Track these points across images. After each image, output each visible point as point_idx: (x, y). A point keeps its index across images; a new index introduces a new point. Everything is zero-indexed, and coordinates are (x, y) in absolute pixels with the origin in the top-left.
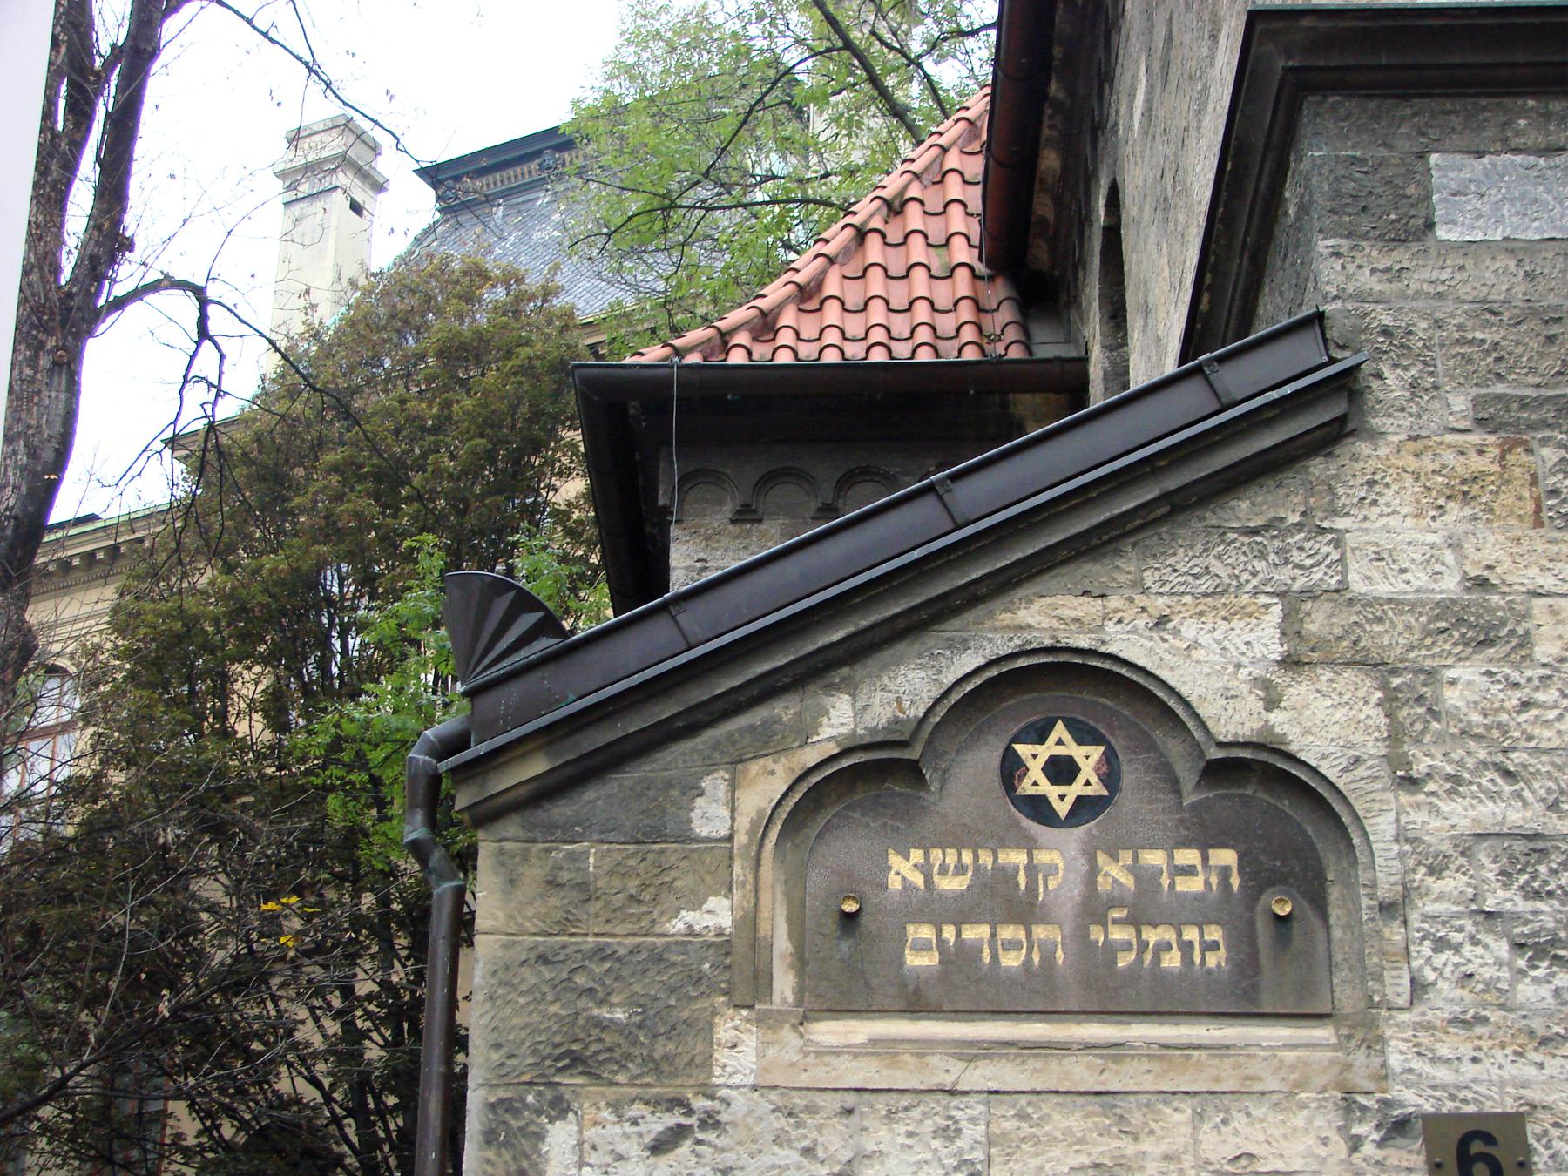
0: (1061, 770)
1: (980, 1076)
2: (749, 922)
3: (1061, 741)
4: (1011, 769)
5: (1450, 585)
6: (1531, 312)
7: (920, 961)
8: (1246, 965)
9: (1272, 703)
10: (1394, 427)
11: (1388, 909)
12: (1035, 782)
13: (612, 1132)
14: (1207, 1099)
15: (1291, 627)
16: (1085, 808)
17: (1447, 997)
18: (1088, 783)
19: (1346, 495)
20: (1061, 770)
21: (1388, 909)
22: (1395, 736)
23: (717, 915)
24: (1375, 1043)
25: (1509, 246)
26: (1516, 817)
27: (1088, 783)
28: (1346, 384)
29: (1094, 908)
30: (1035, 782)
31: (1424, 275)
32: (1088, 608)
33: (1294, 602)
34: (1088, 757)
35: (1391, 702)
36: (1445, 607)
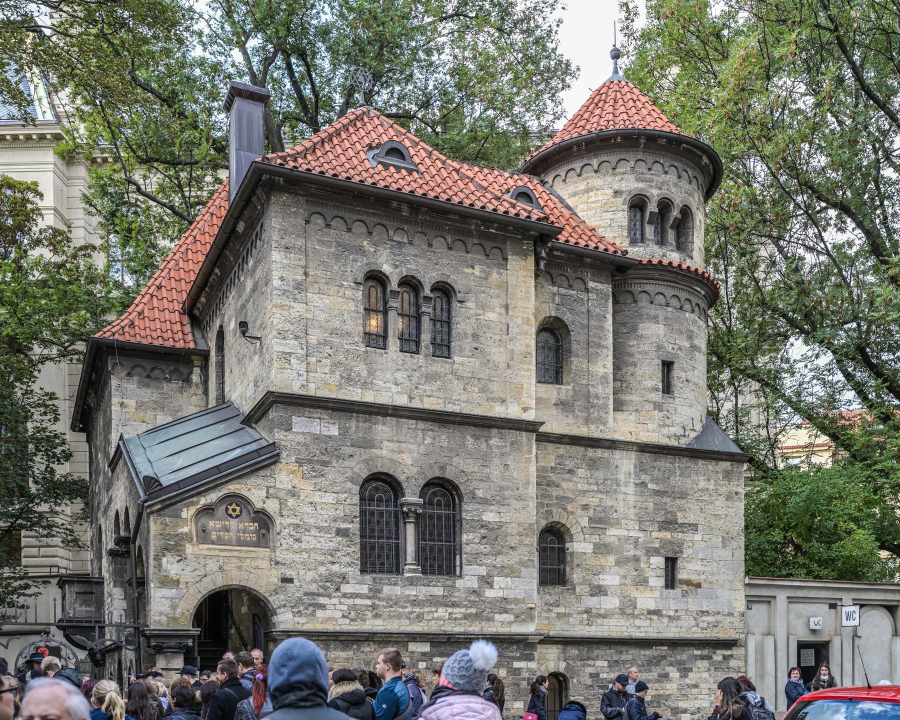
5: (290, 487)
6: (305, 444)
8: (259, 539)
9: (264, 503)
11: (278, 534)
14: (253, 559)
15: (267, 492)
17: (285, 546)
21: (278, 534)
22: (281, 509)
24: (275, 552)
25: (303, 433)
26: (296, 522)
31: (290, 437)
33: (268, 488)
35: (280, 504)
36: (289, 490)
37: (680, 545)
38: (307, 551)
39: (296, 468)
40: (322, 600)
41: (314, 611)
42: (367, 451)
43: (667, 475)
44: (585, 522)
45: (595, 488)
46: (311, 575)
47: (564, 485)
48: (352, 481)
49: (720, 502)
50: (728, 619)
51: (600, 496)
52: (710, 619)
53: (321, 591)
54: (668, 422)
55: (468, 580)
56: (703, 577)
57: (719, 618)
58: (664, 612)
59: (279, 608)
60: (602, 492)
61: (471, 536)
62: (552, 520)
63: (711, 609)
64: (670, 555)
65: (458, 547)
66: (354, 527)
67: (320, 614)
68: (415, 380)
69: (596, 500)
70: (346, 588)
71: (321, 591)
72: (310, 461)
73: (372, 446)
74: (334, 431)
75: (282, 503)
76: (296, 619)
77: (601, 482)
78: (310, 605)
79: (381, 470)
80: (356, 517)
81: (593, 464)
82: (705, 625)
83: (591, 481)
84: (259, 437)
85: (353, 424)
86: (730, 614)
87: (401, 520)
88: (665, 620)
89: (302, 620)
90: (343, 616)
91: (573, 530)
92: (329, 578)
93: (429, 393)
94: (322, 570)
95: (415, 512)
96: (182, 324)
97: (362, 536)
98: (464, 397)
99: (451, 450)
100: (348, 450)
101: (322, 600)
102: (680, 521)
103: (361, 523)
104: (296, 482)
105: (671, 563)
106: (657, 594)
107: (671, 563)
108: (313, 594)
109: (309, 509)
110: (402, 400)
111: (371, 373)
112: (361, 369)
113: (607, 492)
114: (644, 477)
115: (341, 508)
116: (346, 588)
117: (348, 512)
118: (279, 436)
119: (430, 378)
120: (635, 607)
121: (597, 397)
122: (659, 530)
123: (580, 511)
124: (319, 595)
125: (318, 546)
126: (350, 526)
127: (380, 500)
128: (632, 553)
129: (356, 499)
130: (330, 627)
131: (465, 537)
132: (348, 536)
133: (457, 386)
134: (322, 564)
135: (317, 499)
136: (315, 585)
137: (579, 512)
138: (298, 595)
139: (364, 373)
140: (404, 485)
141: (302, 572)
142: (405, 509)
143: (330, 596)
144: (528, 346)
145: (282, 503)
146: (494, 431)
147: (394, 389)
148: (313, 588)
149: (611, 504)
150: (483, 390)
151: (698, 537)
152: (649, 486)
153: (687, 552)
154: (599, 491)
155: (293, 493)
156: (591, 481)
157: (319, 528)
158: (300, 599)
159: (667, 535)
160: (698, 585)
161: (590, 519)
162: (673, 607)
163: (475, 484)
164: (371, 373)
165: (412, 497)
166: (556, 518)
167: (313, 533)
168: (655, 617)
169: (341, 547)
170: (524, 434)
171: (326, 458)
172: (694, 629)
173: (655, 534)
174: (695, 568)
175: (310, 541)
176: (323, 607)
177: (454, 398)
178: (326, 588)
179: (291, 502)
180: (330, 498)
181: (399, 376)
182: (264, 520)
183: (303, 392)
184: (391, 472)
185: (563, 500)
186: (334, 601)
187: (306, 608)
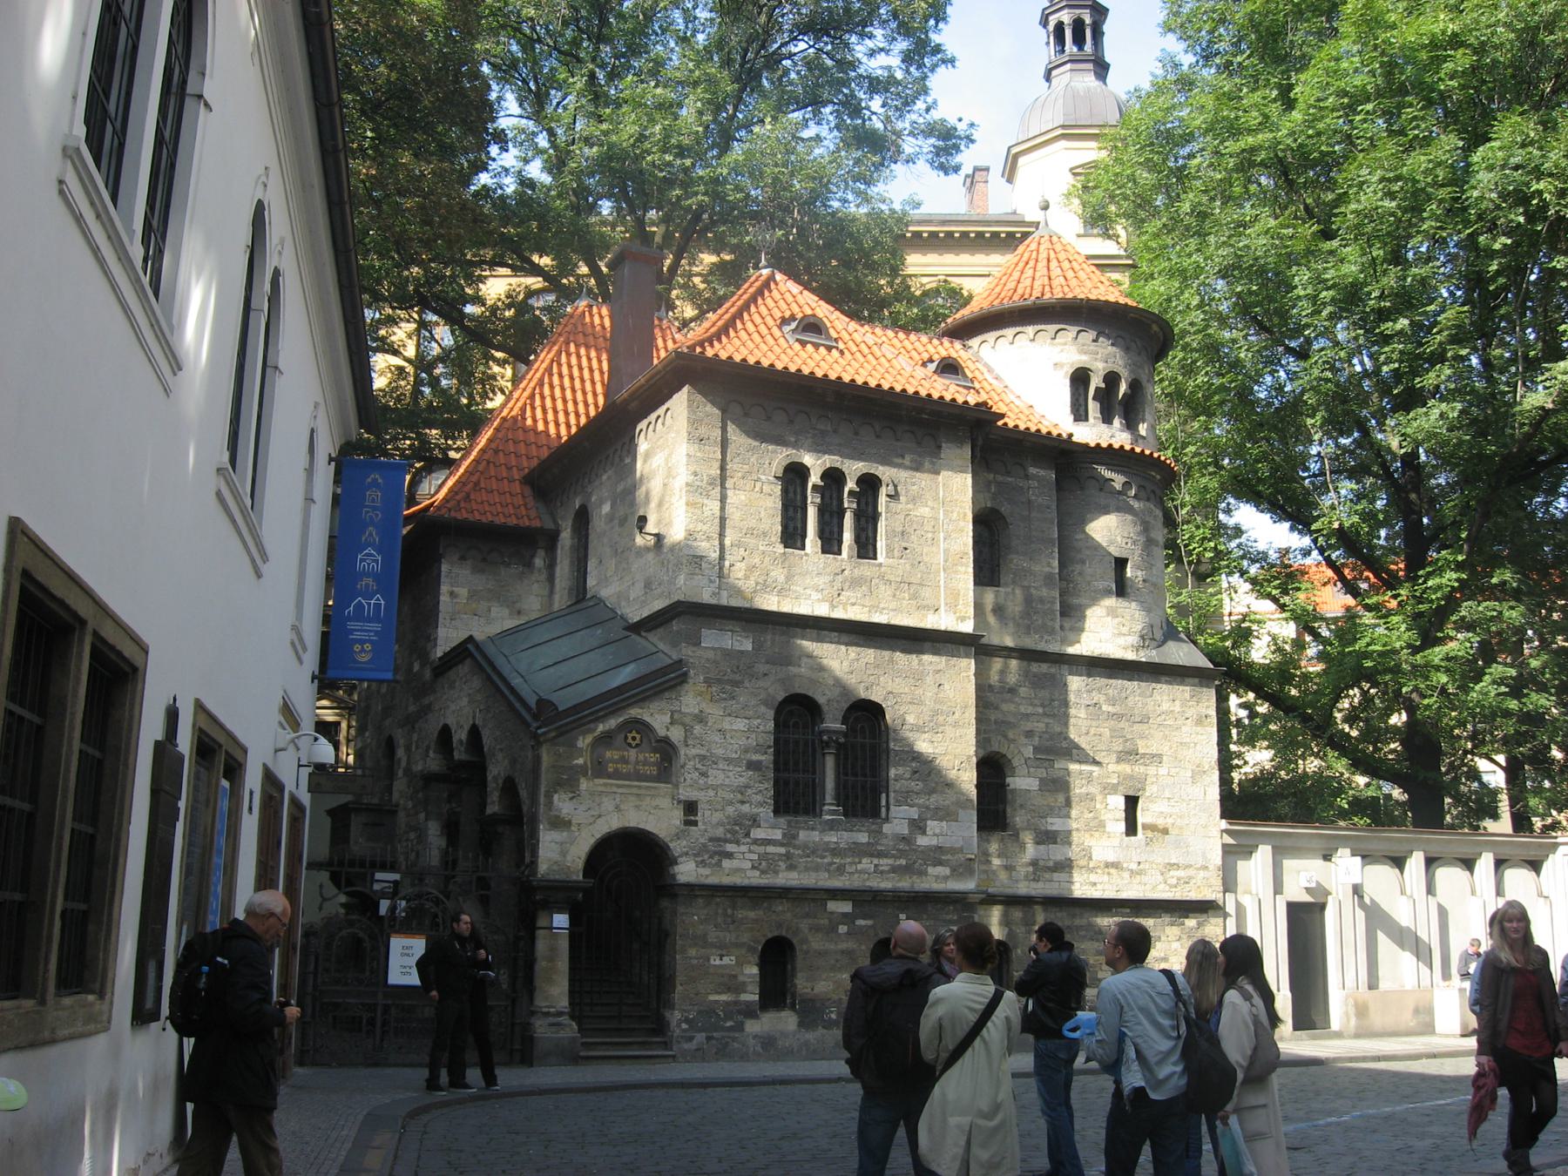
0: (634, 738)
1: (620, 790)
2: (585, 763)
3: (634, 734)
4: (626, 738)
5: (697, 711)
7: (610, 770)
8: (659, 774)
10: (691, 681)
12: (630, 740)
13: (564, 796)
15: (672, 717)
16: (637, 745)
17: (688, 783)
18: (638, 741)
19: (683, 693)
20: (634, 738)
23: (580, 761)
25: (713, 649)
27: (638, 741)
28: (685, 674)
29: (637, 763)
30: (630, 740)
31: (699, 653)
32: (640, 711)
34: (638, 736)
36: (696, 715)
37: (1143, 780)
38: (715, 788)
39: (704, 689)
40: (730, 847)
41: (720, 861)
42: (784, 668)
43: (1124, 695)
44: (1028, 752)
45: (1040, 710)
46: (717, 816)
47: (1005, 707)
48: (765, 703)
49: (1188, 728)
50: (1202, 874)
51: (1046, 720)
52: (1181, 873)
53: (729, 836)
54: (1125, 630)
55: (898, 820)
56: (1170, 821)
57: (1191, 872)
58: (1125, 865)
59: (680, 856)
60: (1048, 716)
61: (901, 770)
62: (989, 749)
63: (1181, 861)
64: (1131, 793)
65: (884, 783)
66: (767, 758)
67: (726, 863)
68: (838, 585)
69: (1041, 726)
70: (758, 833)
71: (729, 836)
72: (719, 681)
73: (789, 664)
74: (748, 646)
75: (688, 730)
76: (703, 871)
77: (1047, 703)
78: (716, 853)
79: (799, 691)
80: (769, 747)
81: (1038, 682)
82: (1174, 881)
83: (1036, 702)
84: (655, 650)
85: (769, 637)
86: (1205, 868)
87: (819, 750)
88: (1126, 875)
89: (707, 871)
90: (753, 867)
91: (1015, 762)
92: (738, 821)
93: (853, 600)
94: (730, 810)
95: (836, 742)
96: (523, 497)
97: (777, 770)
98: (893, 605)
99: (878, 666)
100: (761, 668)
101: (730, 847)
102: (1141, 751)
103: (777, 754)
104: (704, 705)
105: (1132, 802)
106: (1116, 842)
107: (1132, 802)
108: (718, 840)
109: (717, 738)
110: (822, 610)
111: (789, 578)
112: (778, 574)
113: (1054, 716)
114: (1097, 697)
115: (753, 736)
116: (758, 833)
117: (761, 741)
118: (686, 652)
119: (856, 583)
120: (1090, 858)
121: (1041, 600)
122: (1118, 762)
123: (1023, 738)
124: (726, 841)
125: (727, 782)
126: (763, 758)
127: (796, 725)
128: (1083, 790)
129: (771, 725)
130: (738, 880)
131: (893, 772)
132: (760, 770)
133: (884, 592)
134: (731, 803)
135: (726, 726)
136: (721, 829)
137: (1023, 740)
138: (702, 841)
139: (782, 579)
140: (825, 708)
141: (708, 813)
142: (825, 738)
143: (738, 843)
144: (965, 545)
145: (688, 730)
146: (927, 645)
147: (815, 596)
148: (720, 832)
149: (1058, 730)
150: (914, 597)
151: (1163, 771)
152: (1104, 708)
153: (1151, 790)
154: (1045, 714)
155: (701, 718)
156: (1036, 702)
157: (729, 761)
158: (704, 845)
159: (1126, 768)
160: (1165, 831)
161: (1036, 749)
162: (1136, 859)
163: (903, 709)
164: (789, 578)
165: (833, 723)
166: (995, 748)
167: (721, 766)
168: (1113, 871)
169: (752, 783)
170: (962, 648)
171: (737, 677)
172: (1162, 886)
173: (1112, 767)
174: (1163, 809)
175: (717, 776)
176: (730, 855)
177: (882, 605)
178: (734, 833)
179: (698, 729)
180: (740, 724)
181: (822, 581)
182: (666, 750)
183: (714, 601)
184: (810, 694)
185: (1003, 725)
186: (744, 848)
187: (711, 857)
